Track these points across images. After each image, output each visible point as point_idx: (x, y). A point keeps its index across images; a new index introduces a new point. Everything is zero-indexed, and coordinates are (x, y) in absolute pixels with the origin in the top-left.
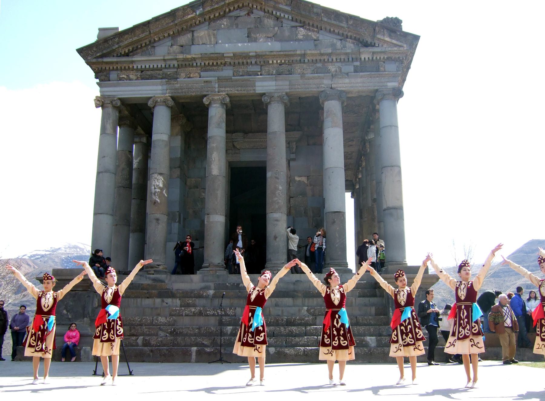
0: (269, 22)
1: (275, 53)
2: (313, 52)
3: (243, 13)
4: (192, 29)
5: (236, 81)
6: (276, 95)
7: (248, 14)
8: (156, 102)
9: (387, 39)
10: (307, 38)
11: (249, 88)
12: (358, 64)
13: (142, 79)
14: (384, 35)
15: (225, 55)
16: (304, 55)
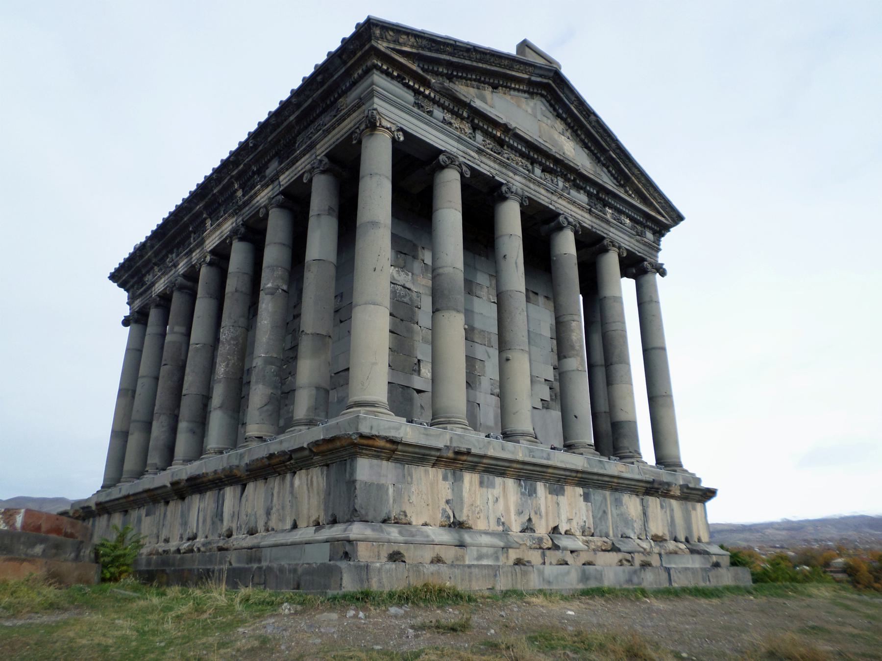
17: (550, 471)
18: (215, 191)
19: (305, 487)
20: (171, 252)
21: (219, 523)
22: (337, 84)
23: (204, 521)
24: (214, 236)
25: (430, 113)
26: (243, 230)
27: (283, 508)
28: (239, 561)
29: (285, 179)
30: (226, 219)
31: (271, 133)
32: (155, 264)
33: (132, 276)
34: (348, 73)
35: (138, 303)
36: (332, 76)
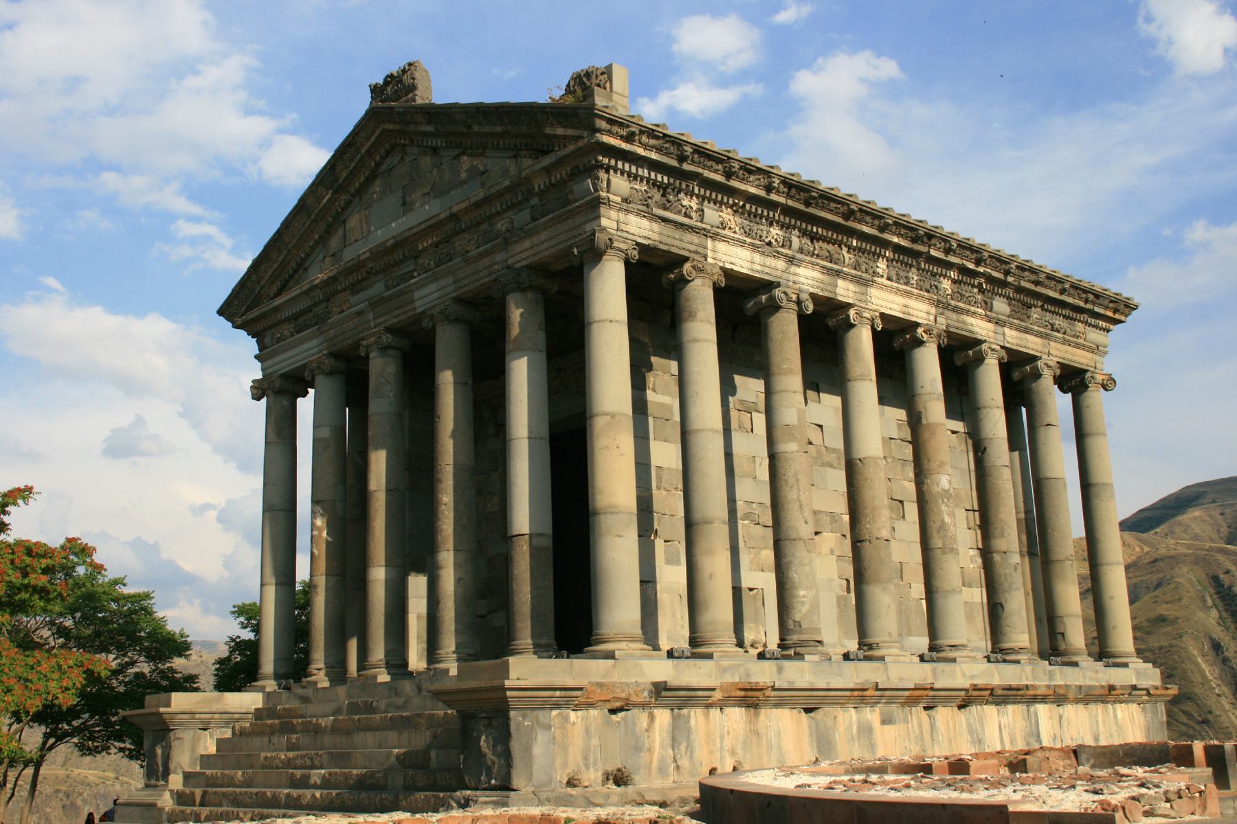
0: (427, 161)
1: (415, 230)
2: (462, 206)
3: (393, 160)
4: (342, 218)
5: (390, 298)
6: (438, 309)
7: (402, 159)
8: (312, 371)
9: (560, 131)
10: (473, 173)
11: (410, 307)
12: (535, 201)
13: (298, 332)
14: (552, 125)
15: (362, 258)
16: (454, 217)
18: (933, 252)
23: (1012, 741)
29: (1013, 338)
36: (1094, 304)
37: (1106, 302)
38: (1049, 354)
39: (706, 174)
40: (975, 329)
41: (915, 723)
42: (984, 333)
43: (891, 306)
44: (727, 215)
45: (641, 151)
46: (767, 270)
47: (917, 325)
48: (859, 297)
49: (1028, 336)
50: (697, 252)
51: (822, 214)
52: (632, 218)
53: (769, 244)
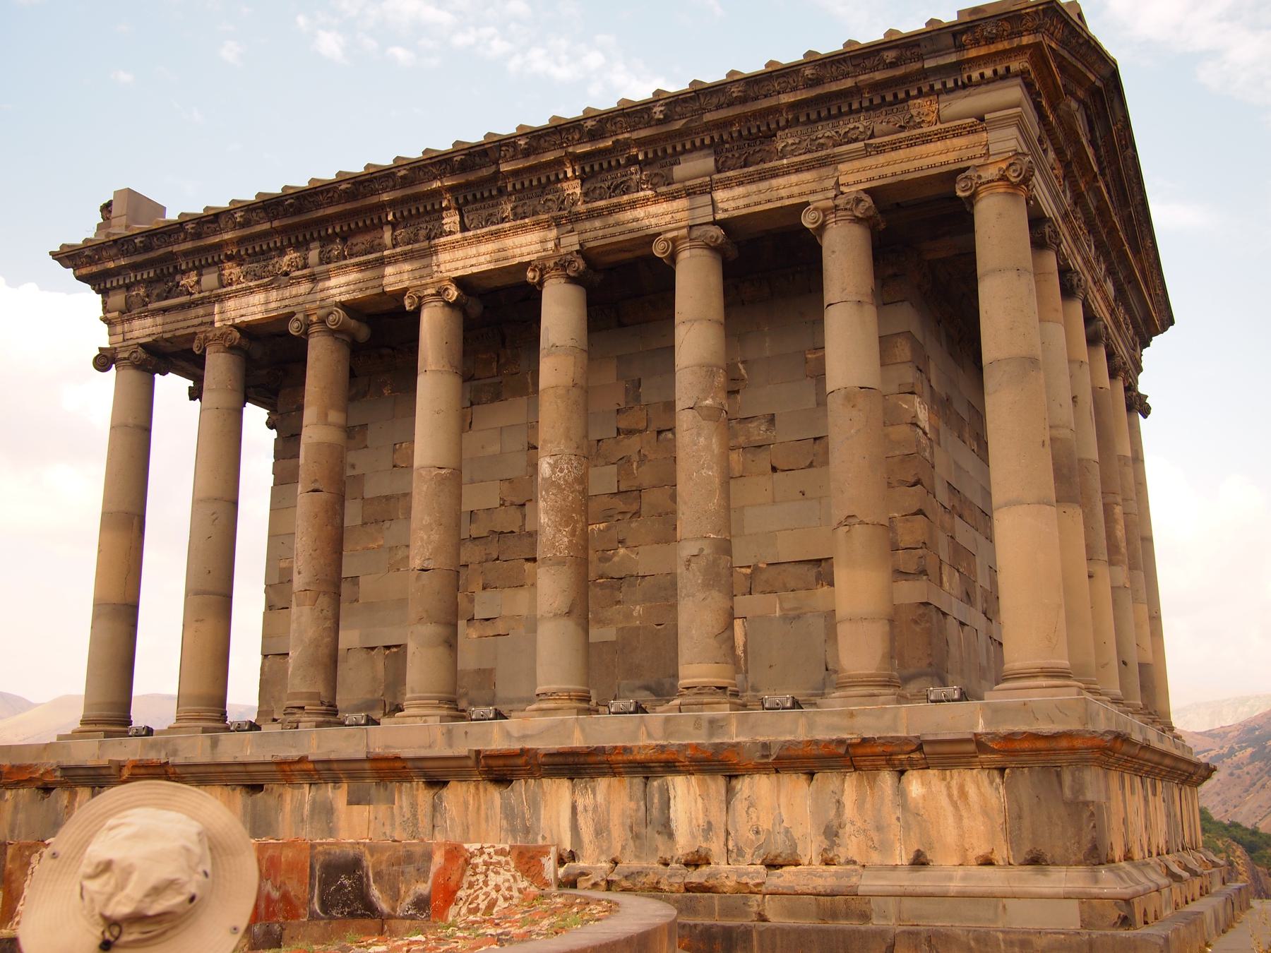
17: (1167, 761)
18: (505, 168)
19: (944, 801)
20: (302, 245)
21: (660, 840)
22: (925, 74)
23: (601, 830)
24: (472, 251)
25: (1045, 151)
26: (580, 264)
27: (879, 828)
28: (792, 913)
29: (733, 200)
30: (524, 229)
31: (719, 107)
32: (230, 258)
33: (135, 267)
34: (958, 66)
35: (144, 329)
36: (921, 58)
37: (950, 41)
38: (837, 183)
39: (176, 248)
40: (646, 222)
41: (405, 802)
42: (668, 218)
43: (473, 261)
44: (232, 270)
45: (111, 265)
46: (287, 302)
47: (529, 263)
48: (417, 274)
49: (775, 182)
50: (202, 324)
51: (321, 213)
52: (137, 323)
53: (286, 274)
